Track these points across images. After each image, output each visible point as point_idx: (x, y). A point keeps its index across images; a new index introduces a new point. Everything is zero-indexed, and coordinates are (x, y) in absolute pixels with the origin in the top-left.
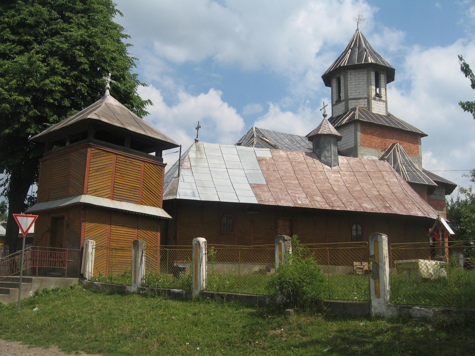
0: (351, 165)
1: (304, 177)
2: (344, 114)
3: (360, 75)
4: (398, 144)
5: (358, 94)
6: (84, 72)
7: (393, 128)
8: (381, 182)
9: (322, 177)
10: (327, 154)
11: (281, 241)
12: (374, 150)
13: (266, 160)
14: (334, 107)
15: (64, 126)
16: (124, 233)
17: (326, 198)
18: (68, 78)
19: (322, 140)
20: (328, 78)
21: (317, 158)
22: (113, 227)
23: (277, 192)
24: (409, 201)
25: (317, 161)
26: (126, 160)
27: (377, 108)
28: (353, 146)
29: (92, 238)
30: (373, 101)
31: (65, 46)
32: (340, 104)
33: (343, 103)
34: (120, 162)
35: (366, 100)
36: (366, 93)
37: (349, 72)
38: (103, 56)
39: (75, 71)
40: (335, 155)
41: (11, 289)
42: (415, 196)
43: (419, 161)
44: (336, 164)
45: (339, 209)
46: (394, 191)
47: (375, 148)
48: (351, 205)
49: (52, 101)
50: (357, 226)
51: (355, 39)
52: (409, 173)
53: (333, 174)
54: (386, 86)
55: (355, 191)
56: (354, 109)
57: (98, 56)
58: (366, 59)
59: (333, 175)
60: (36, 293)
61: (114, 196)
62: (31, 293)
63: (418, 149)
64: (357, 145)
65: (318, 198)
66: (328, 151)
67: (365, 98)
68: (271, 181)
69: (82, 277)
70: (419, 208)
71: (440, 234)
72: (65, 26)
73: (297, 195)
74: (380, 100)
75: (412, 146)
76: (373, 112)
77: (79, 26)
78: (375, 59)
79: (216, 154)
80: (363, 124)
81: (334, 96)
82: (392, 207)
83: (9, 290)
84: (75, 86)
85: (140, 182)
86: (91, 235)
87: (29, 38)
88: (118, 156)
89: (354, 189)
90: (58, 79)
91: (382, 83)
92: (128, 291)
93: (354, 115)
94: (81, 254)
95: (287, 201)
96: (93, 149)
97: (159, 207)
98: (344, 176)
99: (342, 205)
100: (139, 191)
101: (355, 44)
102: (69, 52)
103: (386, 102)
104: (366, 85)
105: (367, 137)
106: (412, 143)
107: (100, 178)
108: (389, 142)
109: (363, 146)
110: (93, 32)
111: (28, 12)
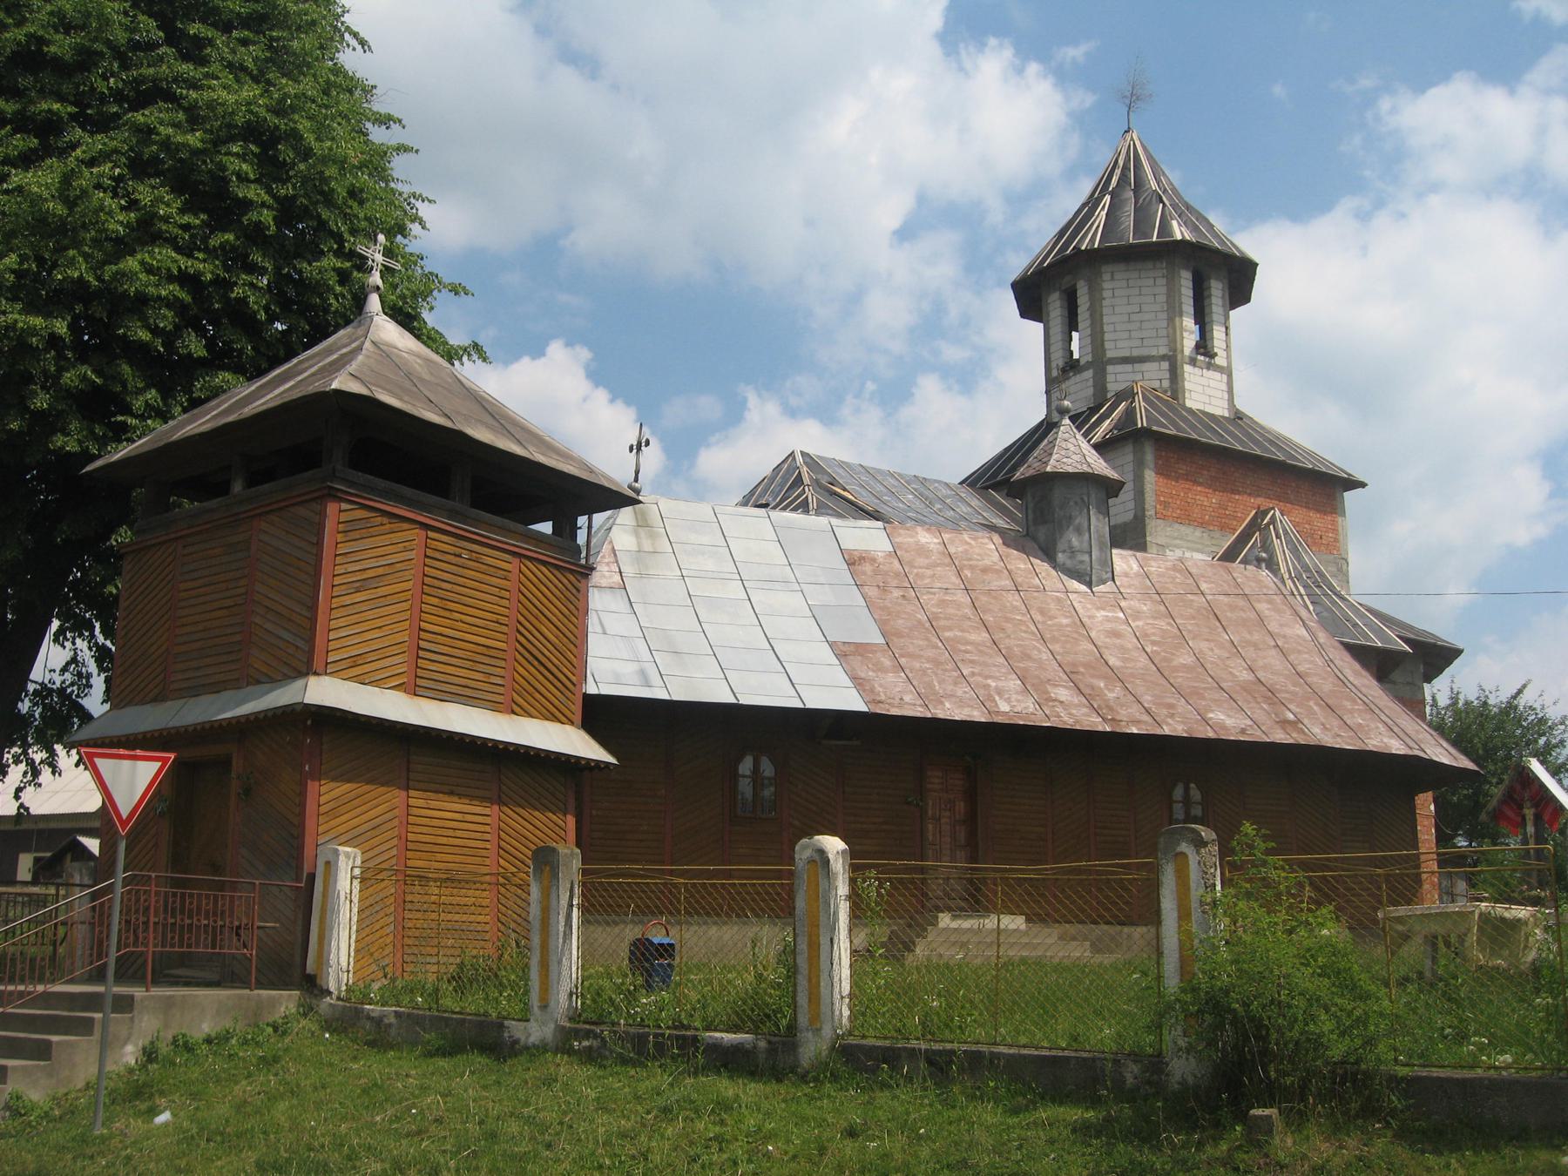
1: (1007, 620)
2: (1093, 410)
5: (1138, 343)
6: (255, 234)
8: (1256, 637)
9: (1065, 621)
10: (1075, 542)
11: (1184, 847)
12: (1198, 533)
13: (873, 560)
15: (231, 418)
16: (457, 819)
17: (1087, 691)
18: (201, 256)
19: (1058, 493)
22: (417, 799)
23: (924, 671)
24: (1354, 701)
25: (1043, 567)
26: (458, 551)
27: (1202, 392)
28: (1129, 516)
29: (343, 839)
30: (1187, 368)
31: (194, 139)
32: (1078, 378)
33: (1089, 374)
34: (437, 555)
35: (1165, 365)
37: (1107, 270)
38: (325, 180)
39: (224, 230)
41: (55, 1038)
43: (1340, 570)
46: (1300, 669)
47: (1202, 524)
48: (1172, 716)
49: (144, 335)
50: (1187, 789)
51: (1121, 163)
52: (1319, 609)
53: (1098, 609)
54: (1227, 317)
55: (1176, 669)
56: (1128, 394)
57: (305, 180)
58: (1165, 228)
60: (150, 1054)
61: (419, 681)
62: (130, 1054)
63: (1335, 531)
65: (1063, 694)
66: (1078, 530)
67: (1164, 358)
68: (899, 635)
69: (312, 985)
70: (1386, 730)
71: (1529, 813)
72: (186, 68)
74: (1210, 366)
75: (1318, 520)
76: (1189, 404)
77: (237, 69)
78: (1195, 229)
79: (705, 540)
81: (1053, 349)
82: (1306, 721)
83: (49, 1043)
84: (223, 285)
85: (504, 629)
86: (342, 829)
87: (56, 106)
88: (430, 534)
89: (1175, 663)
90: (164, 256)
91: (1214, 308)
92: (517, 1042)
93: (1130, 414)
94: (305, 901)
95: (961, 703)
96: (344, 506)
97: (572, 723)
98: (1136, 618)
99: (1146, 718)
100: (502, 664)
101: (1124, 177)
102: (204, 162)
103: (1227, 371)
104: (1165, 316)
105: (1178, 488)
106: (1318, 511)
107: (370, 615)
108: (1246, 507)
109: (1164, 518)
110: (286, 96)
111: (51, 13)
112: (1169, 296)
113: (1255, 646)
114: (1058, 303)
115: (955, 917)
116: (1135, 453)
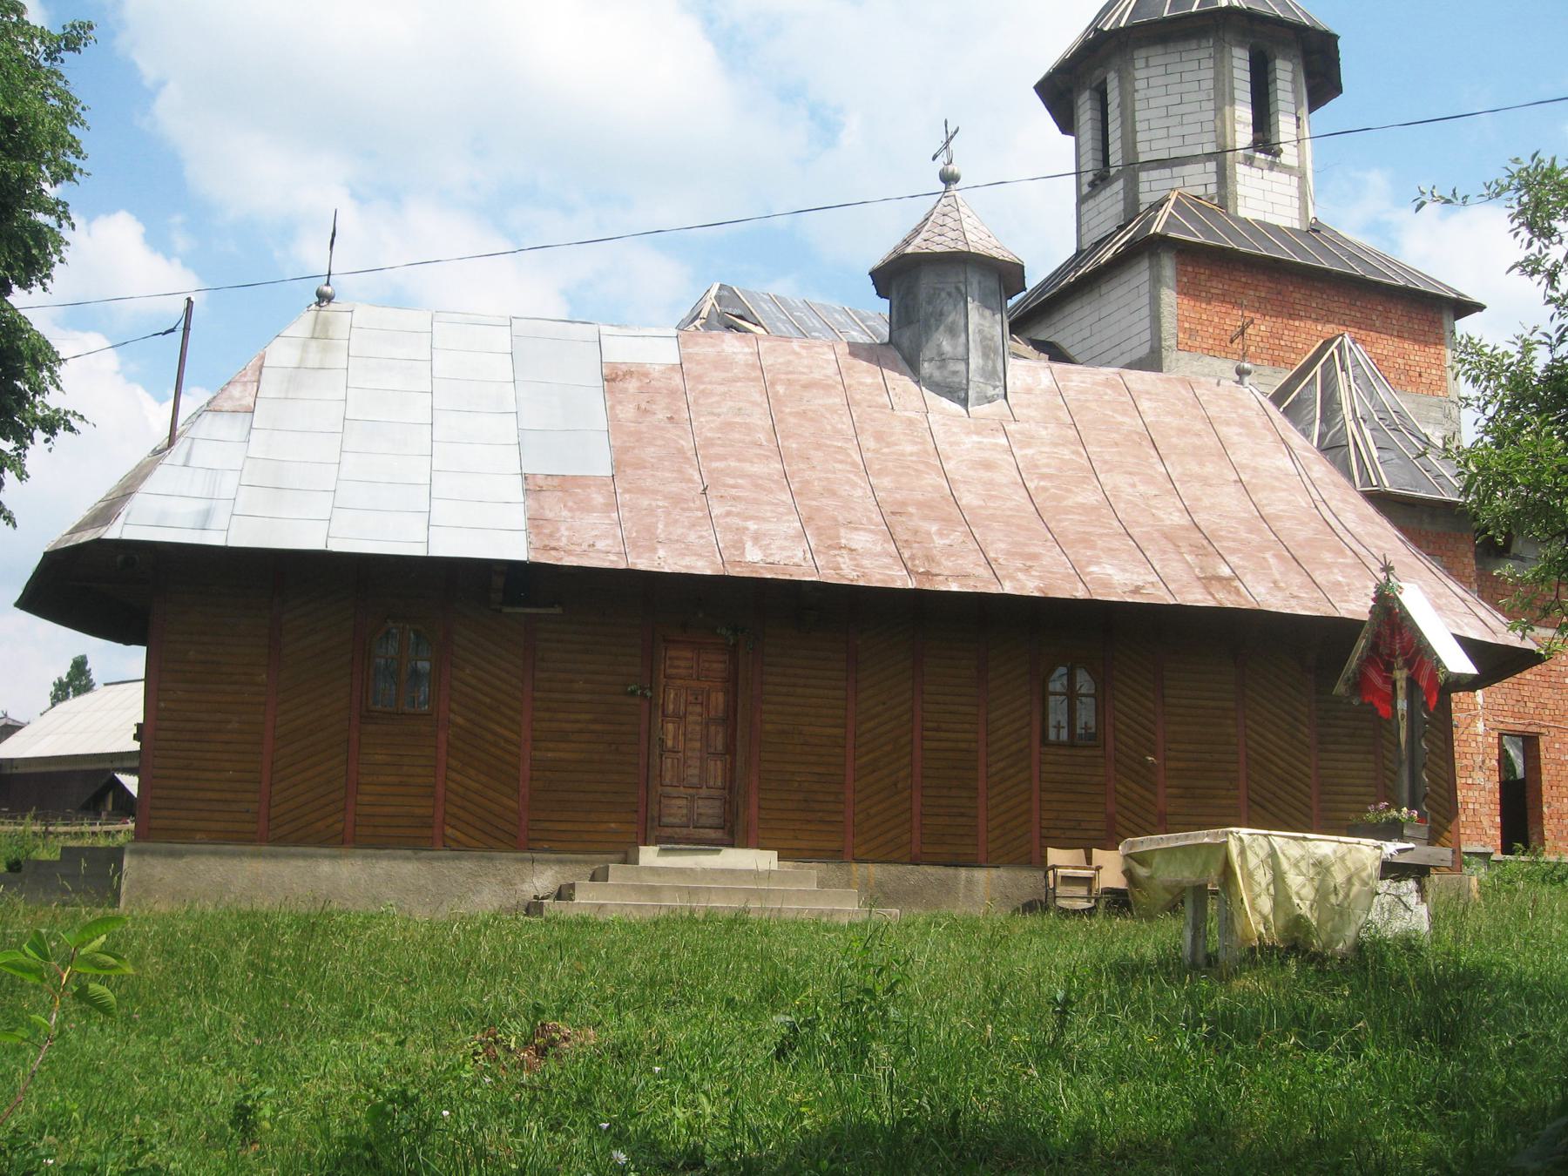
0: (1070, 395)
1: (818, 447)
2: (1121, 228)
3: (1187, 66)
4: (1347, 341)
7: (1327, 272)
8: (1209, 469)
9: (909, 448)
10: (947, 346)
13: (646, 375)
14: (1084, 208)
17: (901, 534)
19: (927, 282)
20: (1063, 91)
21: (903, 365)
24: (1341, 552)
25: (901, 383)
27: (1265, 200)
28: (1145, 349)
30: (1241, 169)
32: (1108, 192)
33: (1118, 185)
35: (1211, 166)
36: (1212, 136)
37: (1140, 58)
40: (987, 351)
42: (1378, 537)
44: (990, 392)
45: (954, 587)
46: (1266, 511)
48: (1028, 569)
52: (1386, 455)
55: (1067, 511)
59: (970, 441)
64: (1160, 347)
66: (952, 332)
67: (1209, 156)
68: (640, 465)
71: (1400, 675)
73: (752, 526)
74: (1272, 166)
75: (1417, 354)
76: (1242, 213)
80: (1188, 253)
82: (1248, 579)
89: (1069, 502)
91: (1280, 95)
95: (688, 550)
99: (984, 572)
104: (1211, 105)
106: (1415, 340)
108: (1307, 334)
112: (1216, 79)
113: (1205, 481)
114: (1088, 105)
115: (664, 852)
116: (1151, 267)
